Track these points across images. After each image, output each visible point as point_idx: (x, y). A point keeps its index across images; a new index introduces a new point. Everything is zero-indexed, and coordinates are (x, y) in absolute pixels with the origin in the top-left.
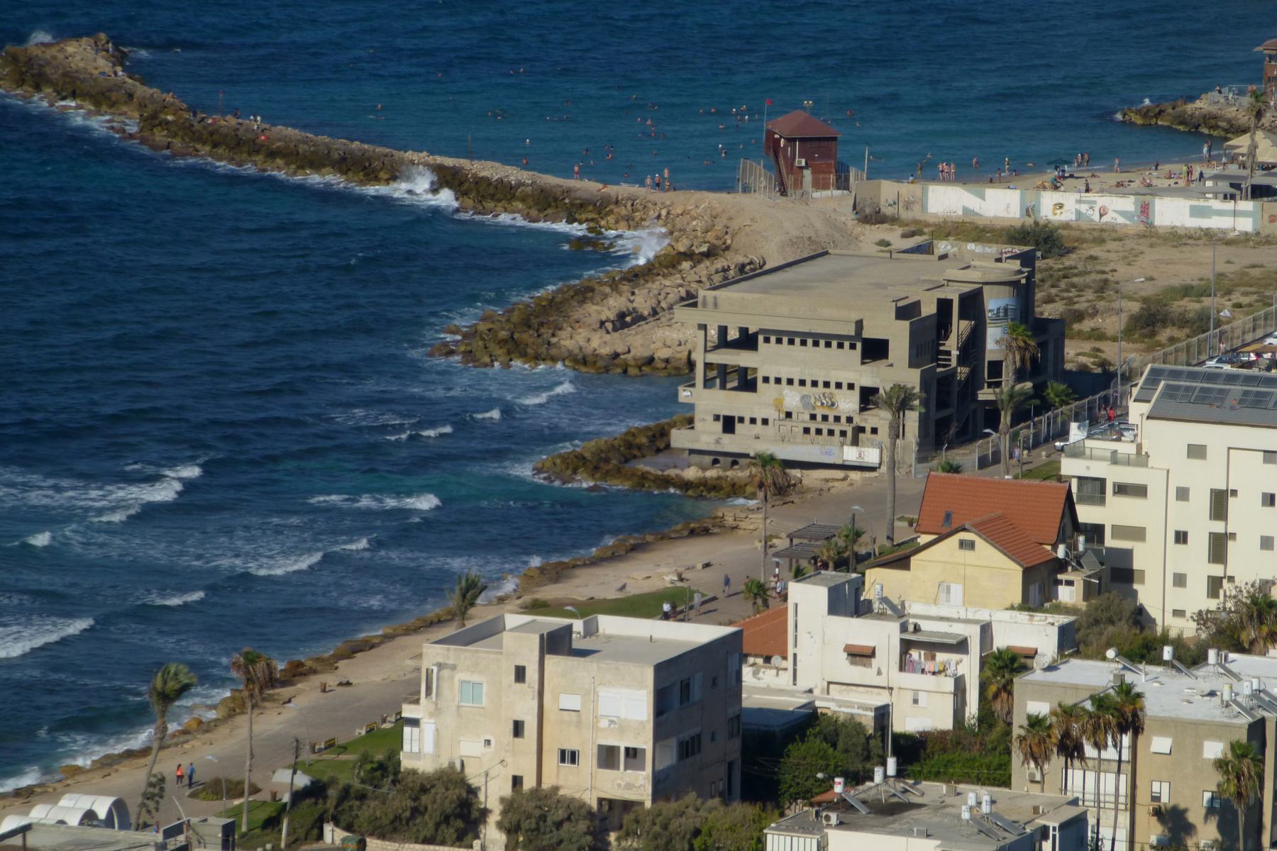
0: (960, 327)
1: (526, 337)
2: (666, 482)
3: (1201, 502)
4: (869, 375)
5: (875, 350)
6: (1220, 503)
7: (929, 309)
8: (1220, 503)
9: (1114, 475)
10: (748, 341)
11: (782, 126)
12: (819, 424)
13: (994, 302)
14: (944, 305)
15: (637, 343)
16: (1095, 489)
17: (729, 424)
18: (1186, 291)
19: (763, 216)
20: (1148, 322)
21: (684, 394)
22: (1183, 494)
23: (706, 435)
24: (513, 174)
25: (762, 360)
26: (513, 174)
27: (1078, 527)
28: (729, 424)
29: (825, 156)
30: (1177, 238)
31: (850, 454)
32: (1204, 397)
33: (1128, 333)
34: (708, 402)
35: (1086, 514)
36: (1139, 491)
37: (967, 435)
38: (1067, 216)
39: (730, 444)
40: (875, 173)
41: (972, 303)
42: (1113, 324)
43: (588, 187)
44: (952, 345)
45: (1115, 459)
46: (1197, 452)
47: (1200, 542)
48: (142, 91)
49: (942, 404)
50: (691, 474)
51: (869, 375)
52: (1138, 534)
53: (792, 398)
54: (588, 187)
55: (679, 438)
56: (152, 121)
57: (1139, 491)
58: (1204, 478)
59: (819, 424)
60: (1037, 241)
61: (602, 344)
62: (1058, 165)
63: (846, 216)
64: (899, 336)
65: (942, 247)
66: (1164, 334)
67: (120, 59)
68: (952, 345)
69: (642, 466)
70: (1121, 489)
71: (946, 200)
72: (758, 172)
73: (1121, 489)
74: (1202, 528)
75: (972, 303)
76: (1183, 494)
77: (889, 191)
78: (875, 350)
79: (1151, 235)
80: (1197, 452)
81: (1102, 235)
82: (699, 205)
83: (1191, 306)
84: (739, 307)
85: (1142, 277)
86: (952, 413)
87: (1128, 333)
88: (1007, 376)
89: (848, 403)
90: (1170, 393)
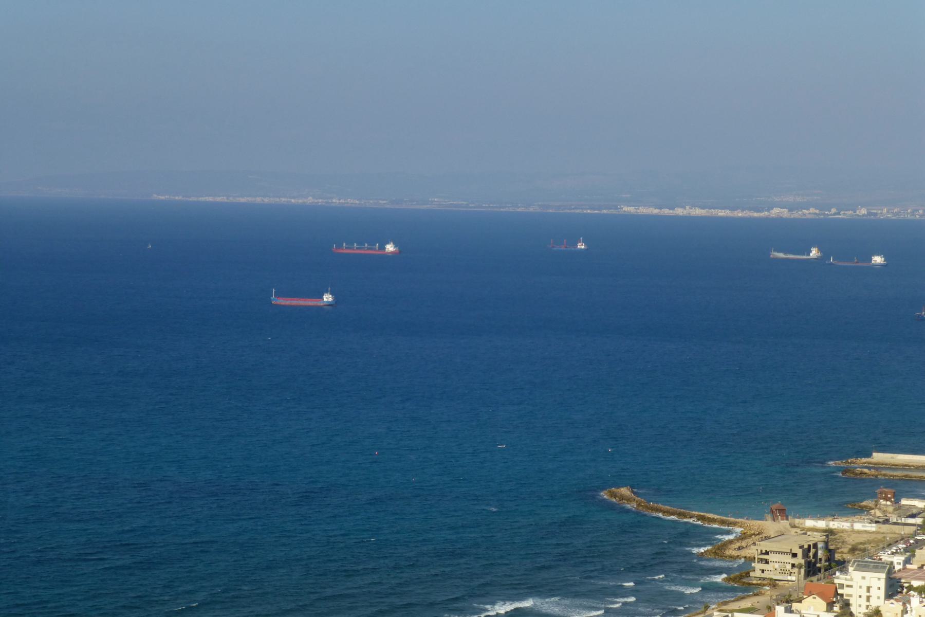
0: (813, 551)
1: (719, 552)
2: (750, 584)
3: (865, 589)
4: (794, 561)
5: (795, 555)
6: (868, 589)
7: (806, 547)
8: (868, 589)
9: (846, 583)
10: (767, 553)
11: (774, 507)
12: (783, 571)
13: (820, 545)
14: (809, 546)
15: (743, 553)
16: (842, 586)
17: (763, 571)
18: (861, 543)
19: (770, 526)
20: (853, 550)
21: (753, 565)
22: (861, 587)
23: (758, 574)
24: (716, 517)
25: (769, 557)
26: (716, 517)
27: (838, 594)
28: (763, 571)
29: (783, 513)
30: (859, 532)
31: (789, 578)
32: (865, 566)
33: (849, 552)
34: (758, 566)
35: (840, 591)
36: (851, 586)
37: (814, 574)
38: (835, 527)
39: (763, 575)
40: (795, 517)
41: (815, 546)
42: (846, 550)
43: (732, 519)
44: (811, 554)
45: (846, 580)
46: (864, 578)
47: (864, 598)
48: (637, 499)
49: (809, 567)
50: (755, 582)
51: (794, 561)
52: (851, 596)
53: (777, 565)
54: (732, 519)
55: (752, 574)
56: (639, 505)
57: (851, 586)
58: (865, 584)
59: (783, 571)
60: (829, 532)
61: (735, 553)
62: (833, 517)
63: (788, 526)
64: (800, 552)
65: (809, 533)
66: (857, 552)
67: (633, 492)
68: (811, 554)
69: (744, 580)
70: (848, 586)
71: (809, 523)
72: (769, 517)
73: (848, 586)
74: (865, 594)
75: (815, 546)
76: (861, 587)
77: (797, 521)
78: (795, 555)
79: (854, 531)
80: (864, 578)
81: (843, 531)
82: (755, 524)
83: (862, 546)
84: (765, 546)
85: (852, 540)
86: (811, 569)
87: (849, 552)
88: (823, 561)
89: (789, 567)
90: (858, 565)
